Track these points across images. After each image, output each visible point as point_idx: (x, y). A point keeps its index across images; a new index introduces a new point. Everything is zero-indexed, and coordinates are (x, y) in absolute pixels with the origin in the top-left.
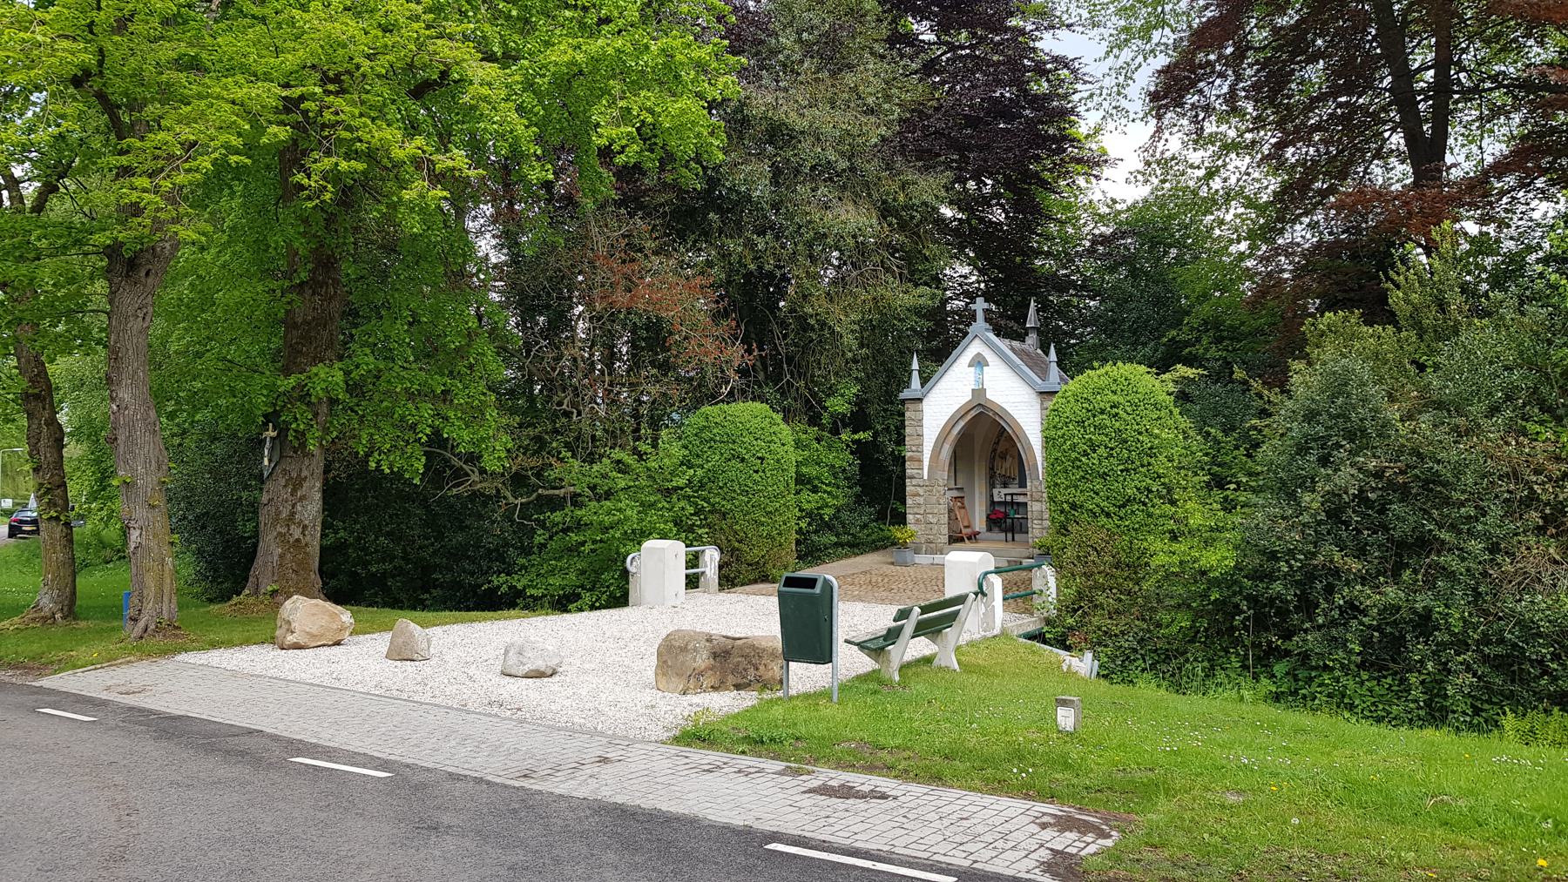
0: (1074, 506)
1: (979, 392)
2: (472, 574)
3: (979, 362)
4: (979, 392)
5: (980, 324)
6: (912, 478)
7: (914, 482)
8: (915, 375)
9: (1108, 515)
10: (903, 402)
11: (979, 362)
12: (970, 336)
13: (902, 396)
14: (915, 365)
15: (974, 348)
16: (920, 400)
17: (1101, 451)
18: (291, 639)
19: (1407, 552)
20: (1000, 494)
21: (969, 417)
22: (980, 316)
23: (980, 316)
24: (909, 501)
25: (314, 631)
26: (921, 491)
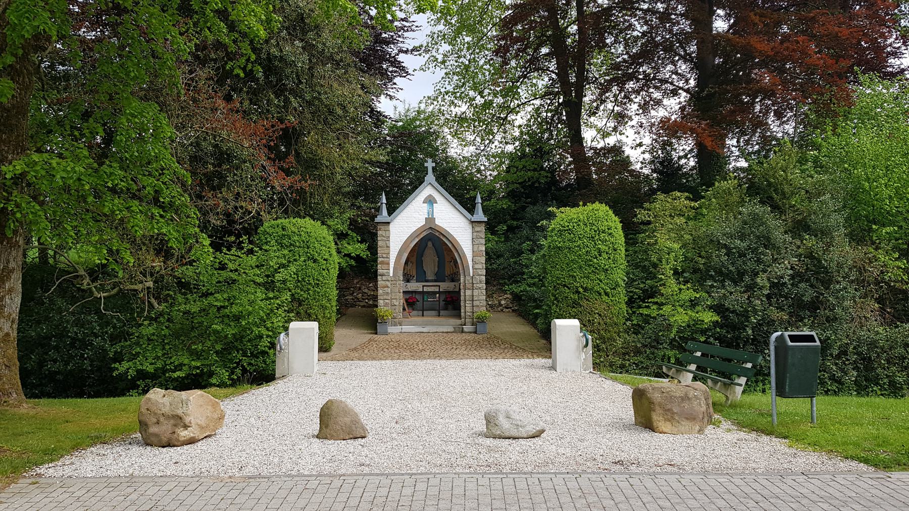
0: (586, 289)
1: (430, 220)
2: (55, 361)
3: (430, 201)
4: (430, 220)
5: (430, 177)
6: (382, 275)
7: (384, 278)
8: (384, 206)
9: (607, 294)
11: (430, 201)
13: (377, 220)
15: (427, 190)
17: (605, 255)
18: (184, 434)
19: (803, 309)
20: (415, 286)
21: (422, 236)
22: (430, 170)
23: (430, 170)
25: (203, 424)
26: (389, 284)
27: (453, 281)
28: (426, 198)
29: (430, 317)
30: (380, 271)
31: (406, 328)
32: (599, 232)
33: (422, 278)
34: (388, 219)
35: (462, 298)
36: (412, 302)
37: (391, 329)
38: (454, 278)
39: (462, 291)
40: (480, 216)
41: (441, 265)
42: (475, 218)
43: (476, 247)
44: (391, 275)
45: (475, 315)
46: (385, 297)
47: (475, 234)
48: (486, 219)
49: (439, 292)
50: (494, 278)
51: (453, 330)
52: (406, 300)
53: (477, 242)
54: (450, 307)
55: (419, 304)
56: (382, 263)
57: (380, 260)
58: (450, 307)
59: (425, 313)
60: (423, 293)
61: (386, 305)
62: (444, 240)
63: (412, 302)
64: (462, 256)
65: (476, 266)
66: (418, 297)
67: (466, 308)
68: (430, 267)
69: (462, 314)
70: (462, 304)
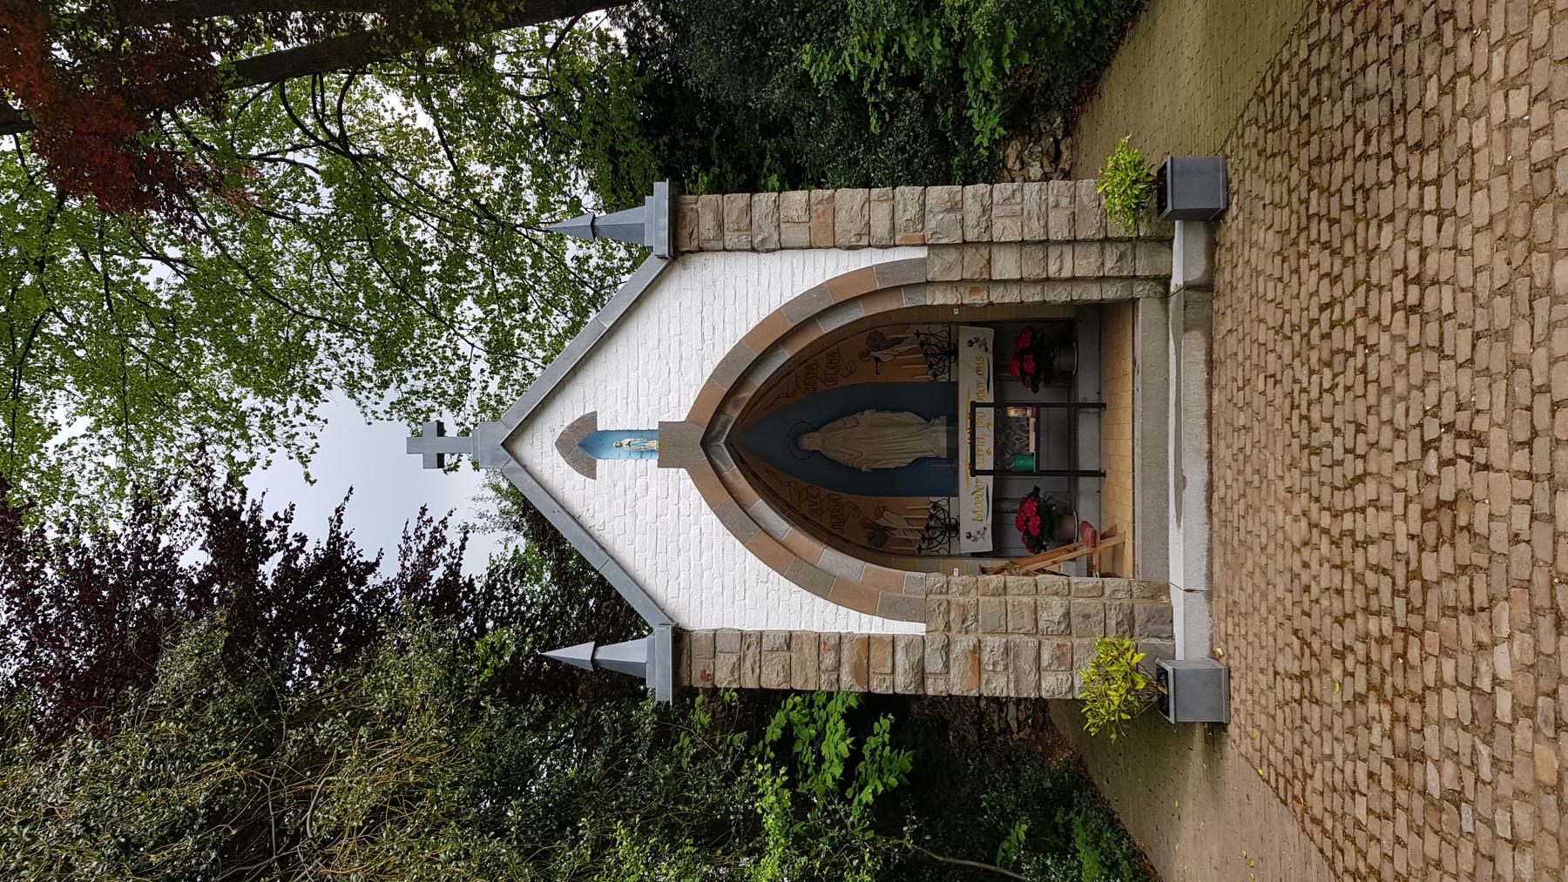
1: (669, 445)
3: (585, 444)
4: (669, 445)
6: (921, 673)
7: (934, 664)
8: (608, 653)
10: (684, 692)
11: (585, 444)
14: (580, 653)
16: (680, 636)
20: (972, 504)
21: (742, 484)
24: (999, 686)
26: (963, 643)
27: (952, 353)
29: (1121, 445)
30: (902, 684)
31: (1183, 563)
33: (939, 475)
34: (662, 637)
35: (1032, 295)
36: (1045, 519)
39: (998, 295)
41: (891, 400)
43: (791, 234)
44: (919, 629)
45: (1117, 228)
46: (1026, 662)
47: (731, 239)
48: (662, 188)
49: (1000, 405)
50: (944, 158)
51: (1195, 343)
52: (1036, 545)
54: (1060, 361)
55: (1046, 486)
56: (863, 670)
58: (1060, 361)
59: (1086, 462)
60: (1001, 473)
61: (1065, 659)
62: (759, 380)
63: (1045, 519)
64: (833, 298)
65: (881, 228)
66: (1019, 489)
67: (1079, 274)
68: (896, 441)
69: (1111, 292)
70: (1060, 295)
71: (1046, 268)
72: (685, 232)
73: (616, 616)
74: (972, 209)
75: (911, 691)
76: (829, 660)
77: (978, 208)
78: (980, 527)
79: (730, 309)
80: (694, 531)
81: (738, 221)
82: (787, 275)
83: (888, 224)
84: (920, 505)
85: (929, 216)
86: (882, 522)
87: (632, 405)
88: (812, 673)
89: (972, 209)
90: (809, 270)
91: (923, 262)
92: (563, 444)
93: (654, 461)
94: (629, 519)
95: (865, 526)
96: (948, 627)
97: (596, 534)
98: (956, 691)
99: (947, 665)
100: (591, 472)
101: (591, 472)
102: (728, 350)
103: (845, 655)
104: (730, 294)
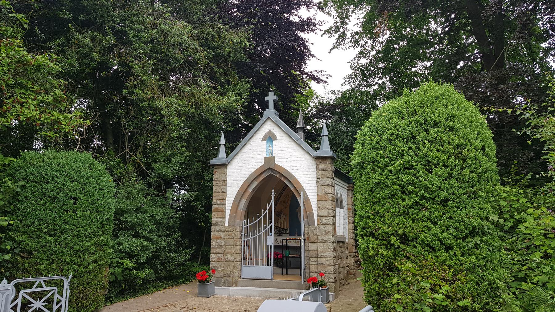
0: (404, 239)
1: (269, 160)
3: (270, 138)
4: (269, 160)
5: (271, 111)
6: (216, 225)
7: (218, 228)
9: (448, 248)
12: (264, 118)
13: (212, 162)
14: (223, 141)
15: (268, 127)
21: (261, 178)
22: (271, 104)
23: (271, 104)
24: (213, 244)
26: (222, 235)
28: (265, 135)
30: (214, 220)
32: (426, 125)
37: (219, 290)
38: (295, 229)
40: (326, 149)
42: (319, 153)
44: (227, 224)
53: (322, 183)
56: (217, 210)
57: (214, 207)
59: (290, 271)
71: (312, 257)
72: (320, 161)
73: (231, 148)
74: (326, 238)
75: (212, 222)
76: (219, 202)
77: (325, 239)
78: (279, 242)
79: (302, 173)
80: (249, 167)
81: (323, 175)
82: (311, 188)
83: (322, 215)
84: (286, 225)
85: (324, 226)
86: (282, 215)
87: (279, 149)
88: (216, 198)
89: (326, 238)
90: (312, 194)
91: (314, 224)
92: (270, 132)
93: (265, 156)
94: (252, 150)
95: (281, 210)
96: (227, 231)
97: (249, 142)
98: (212, 233)
99: (217, 231)
100: (263, 140)
101: (263, 140)
102: (293, 174)
103: (220, 206)
104: (306, 173)
